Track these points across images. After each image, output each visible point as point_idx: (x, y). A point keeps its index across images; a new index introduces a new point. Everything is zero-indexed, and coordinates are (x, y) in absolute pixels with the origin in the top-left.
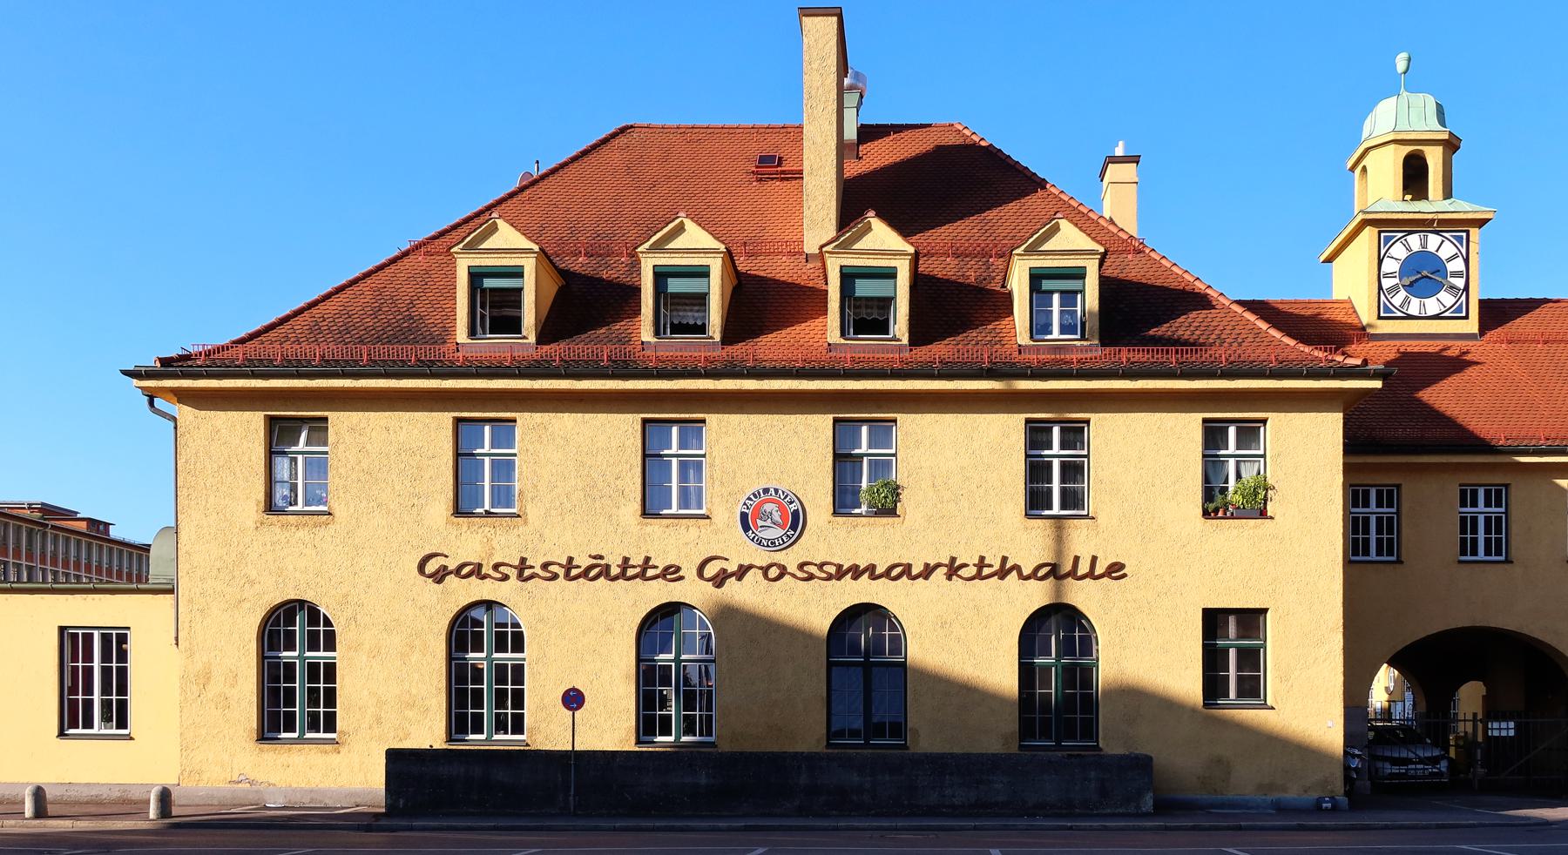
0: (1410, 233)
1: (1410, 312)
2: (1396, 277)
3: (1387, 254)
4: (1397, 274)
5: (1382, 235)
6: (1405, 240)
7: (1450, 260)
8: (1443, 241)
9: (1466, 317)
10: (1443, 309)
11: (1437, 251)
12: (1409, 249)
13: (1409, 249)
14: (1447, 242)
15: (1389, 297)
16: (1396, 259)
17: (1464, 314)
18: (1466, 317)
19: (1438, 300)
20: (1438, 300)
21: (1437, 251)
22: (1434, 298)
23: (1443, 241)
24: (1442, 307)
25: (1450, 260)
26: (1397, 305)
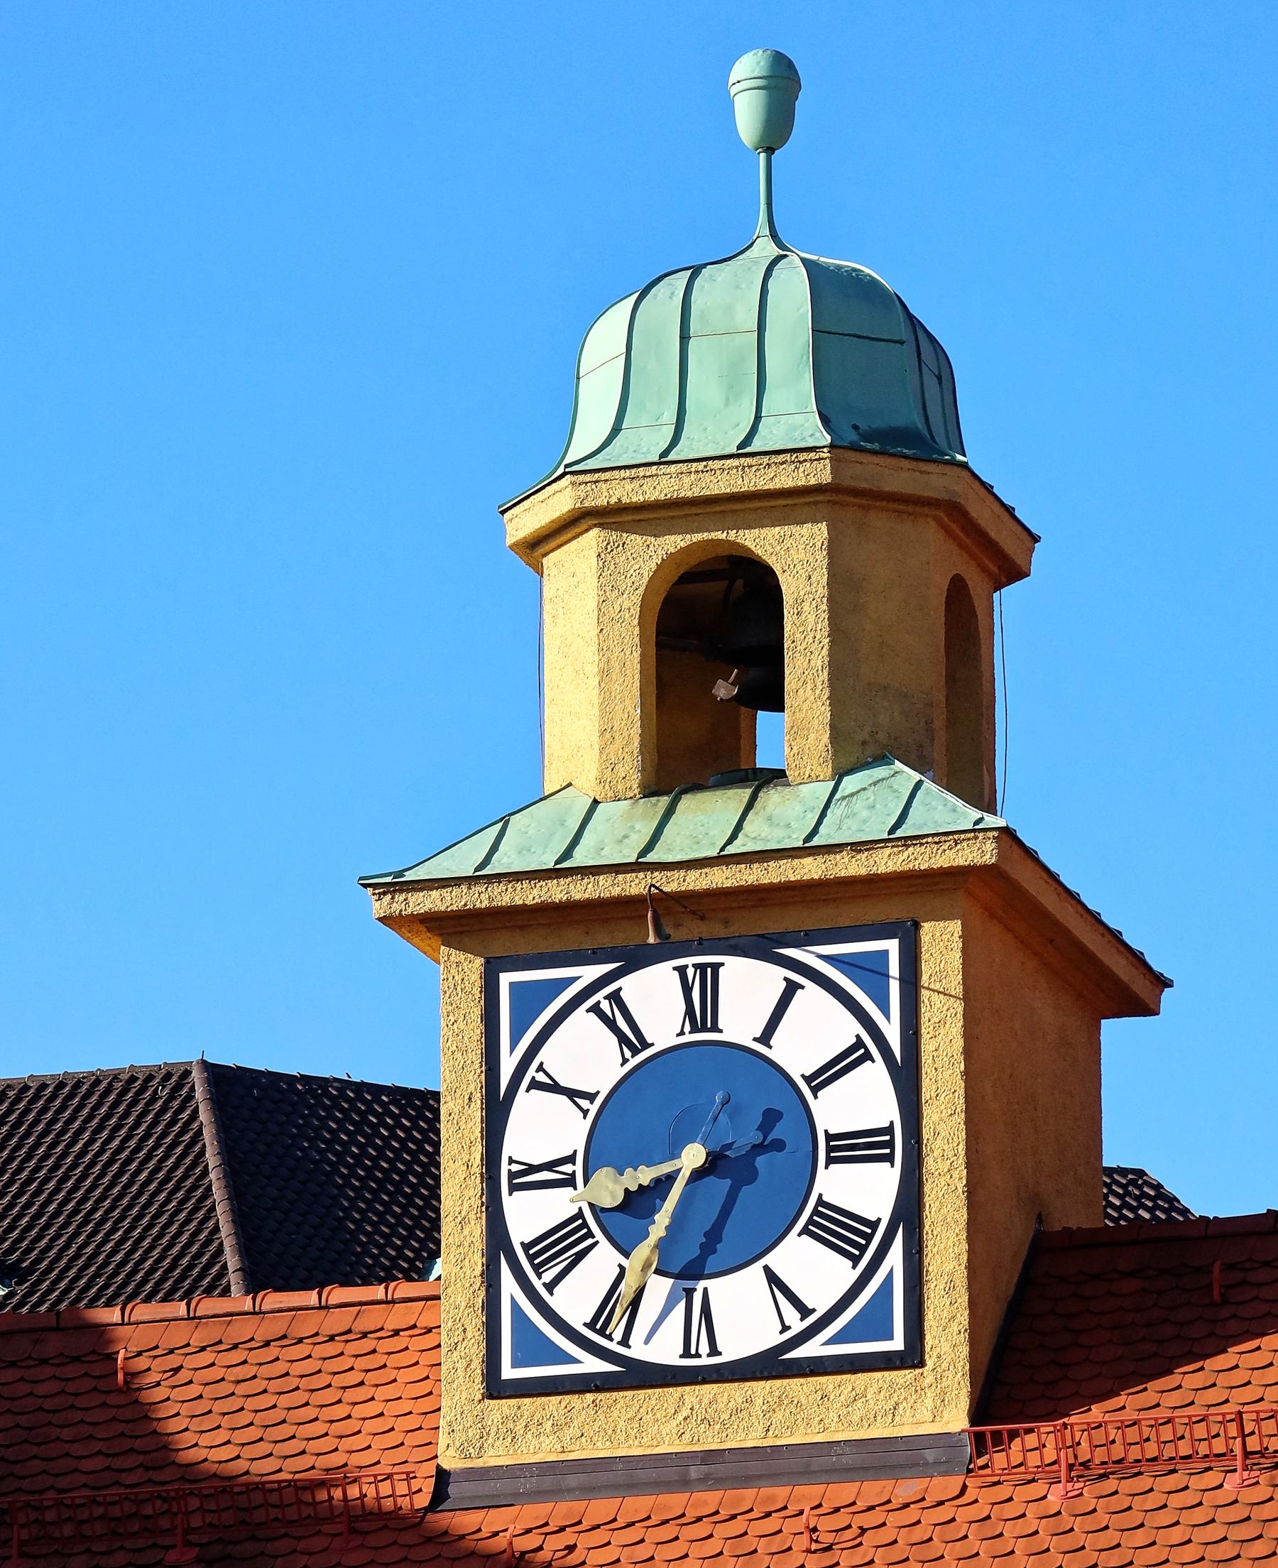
0: (635, 959)
1: (638, 1351)
3: (531, 1072)
4: (579, 1168)
5: (506, 979)
6: (615, 997)
7: (823, 1077)
8: (791, 989)
9: (912, 1357)
10: (797, 1325)
12: (632, 1040)
13: (632, 1040)
14: (810, 993)
15: (538, 1285)
18: (912, 1357)
19: (773, 1279)
20: (773, 1279)
22: (757, 1268)
23: (791, 989)
25: (823, 1077)
26: (578, 1317)
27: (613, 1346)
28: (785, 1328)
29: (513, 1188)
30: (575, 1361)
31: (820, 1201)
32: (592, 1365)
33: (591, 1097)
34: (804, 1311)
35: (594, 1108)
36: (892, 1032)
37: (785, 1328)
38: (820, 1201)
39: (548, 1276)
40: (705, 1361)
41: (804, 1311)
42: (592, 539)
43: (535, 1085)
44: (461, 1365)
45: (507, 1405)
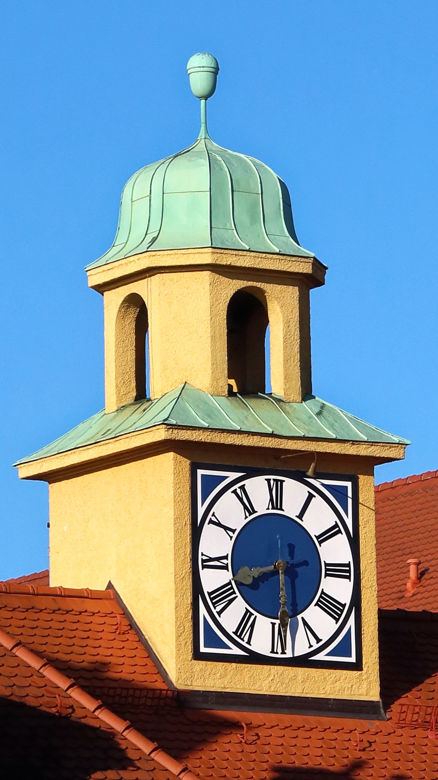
2: (225, 567)
3: (210, 516)
5: (200, 472)
6: (242, 488)
10: (316, 646)
11: (300, 516)
14: (318, 499)
15: (214, 611)
16: (226, 528)
17: (353, 659)
21: (300, 516)
24: (313, 641)
26: (231, 630)
27: (244, 644)
28: (311, 646)
29: (204, 567)
30: (229, 648)
31: (323, 592)
32: (236, 651)
33: (234, 531)
34: (318, 640)
35: (235, 536)
36: (349, 522)
37: (311, 646)
38: (323, 592)
39: (219, 608)
40: (280, 656)
41: (318, 640)
42: (206, 275)
43: (211, 522)
44: (183, 643)
45: (202, 664)
